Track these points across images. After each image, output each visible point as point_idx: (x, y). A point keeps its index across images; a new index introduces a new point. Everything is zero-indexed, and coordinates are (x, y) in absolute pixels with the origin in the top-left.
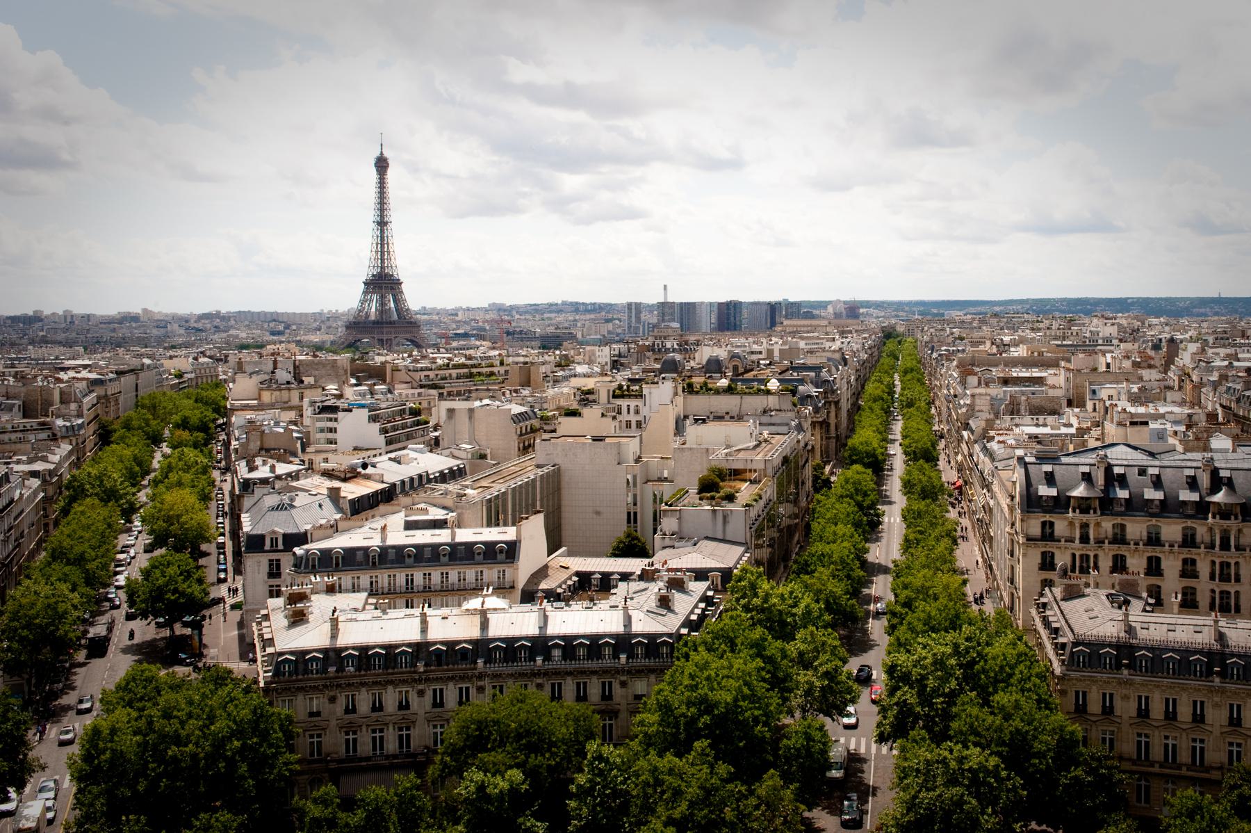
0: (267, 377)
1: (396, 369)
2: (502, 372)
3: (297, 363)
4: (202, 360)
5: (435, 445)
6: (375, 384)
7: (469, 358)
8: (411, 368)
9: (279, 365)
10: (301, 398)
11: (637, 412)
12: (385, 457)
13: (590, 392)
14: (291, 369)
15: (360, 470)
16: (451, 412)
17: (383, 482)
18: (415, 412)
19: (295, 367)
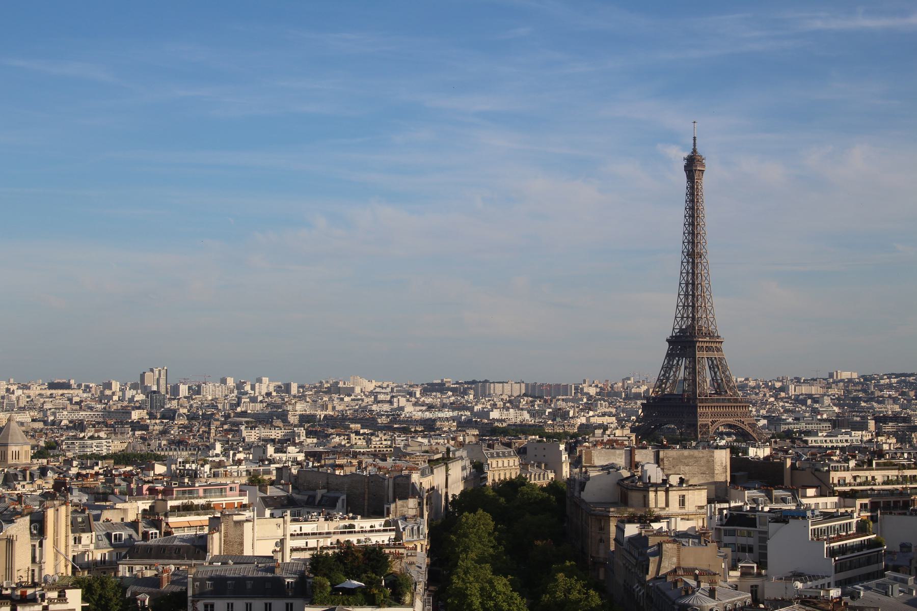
10: (682, 502)
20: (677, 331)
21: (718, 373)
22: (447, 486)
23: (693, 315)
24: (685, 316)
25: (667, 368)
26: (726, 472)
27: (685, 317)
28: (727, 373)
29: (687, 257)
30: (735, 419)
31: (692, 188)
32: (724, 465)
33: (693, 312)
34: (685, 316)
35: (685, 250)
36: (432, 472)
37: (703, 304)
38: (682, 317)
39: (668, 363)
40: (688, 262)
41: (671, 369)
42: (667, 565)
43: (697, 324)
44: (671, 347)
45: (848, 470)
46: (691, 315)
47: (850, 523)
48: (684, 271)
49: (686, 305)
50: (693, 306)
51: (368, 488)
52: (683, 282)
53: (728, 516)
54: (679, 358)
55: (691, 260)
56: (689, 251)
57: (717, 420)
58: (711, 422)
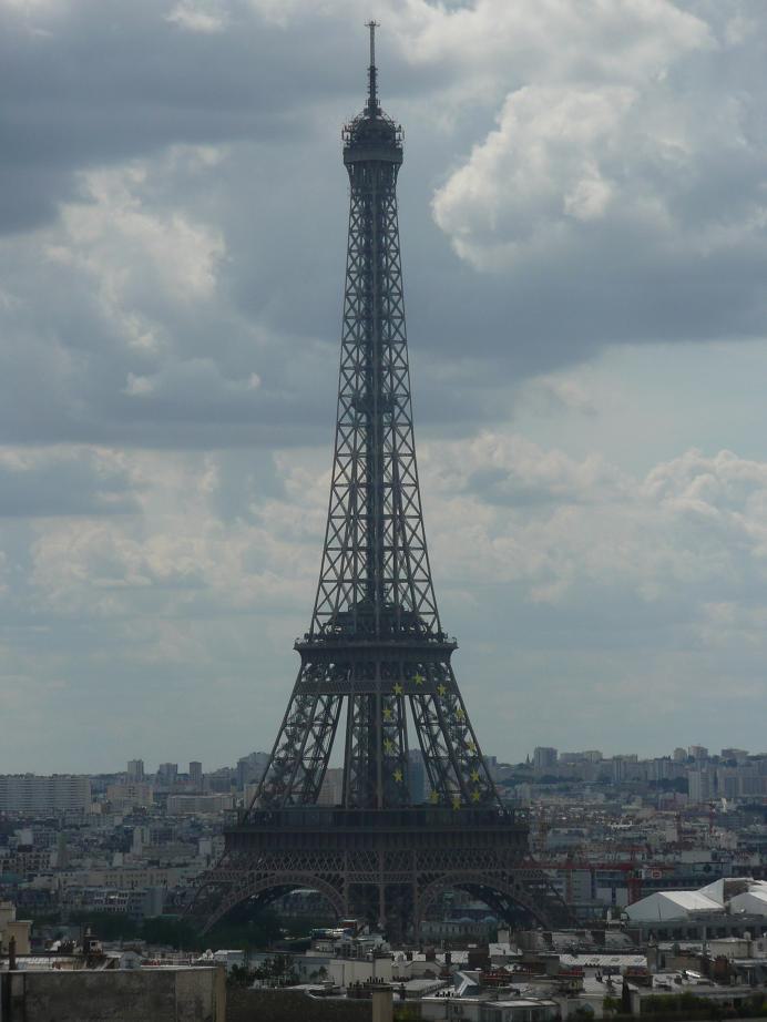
3: (16, 984)
20: (323, 619)
21: (441, 740)
23: (370, 574)
24: (348, 575)
25: (296, 726)
27: (348, 581)
28: (468, 738)
29: (352, 410)
30: (487, 871)
31: (366, 213)
32: (205, 1016)
33: (370, 566)
34: (348, 575)
35: (348, 391)
37: (400, 544)
38: (340, 581)
39: (301, 711)
41: (308, 727)
43: (383, 598)
44: (309, 665)
46: (364, 575)
49: (350, 544)
50: (369, 551)
52: (342, 480)
54: (330, 696)
55: (364, 420)
56: (357, 391)
57: (437, 876)
58: (419, 880)
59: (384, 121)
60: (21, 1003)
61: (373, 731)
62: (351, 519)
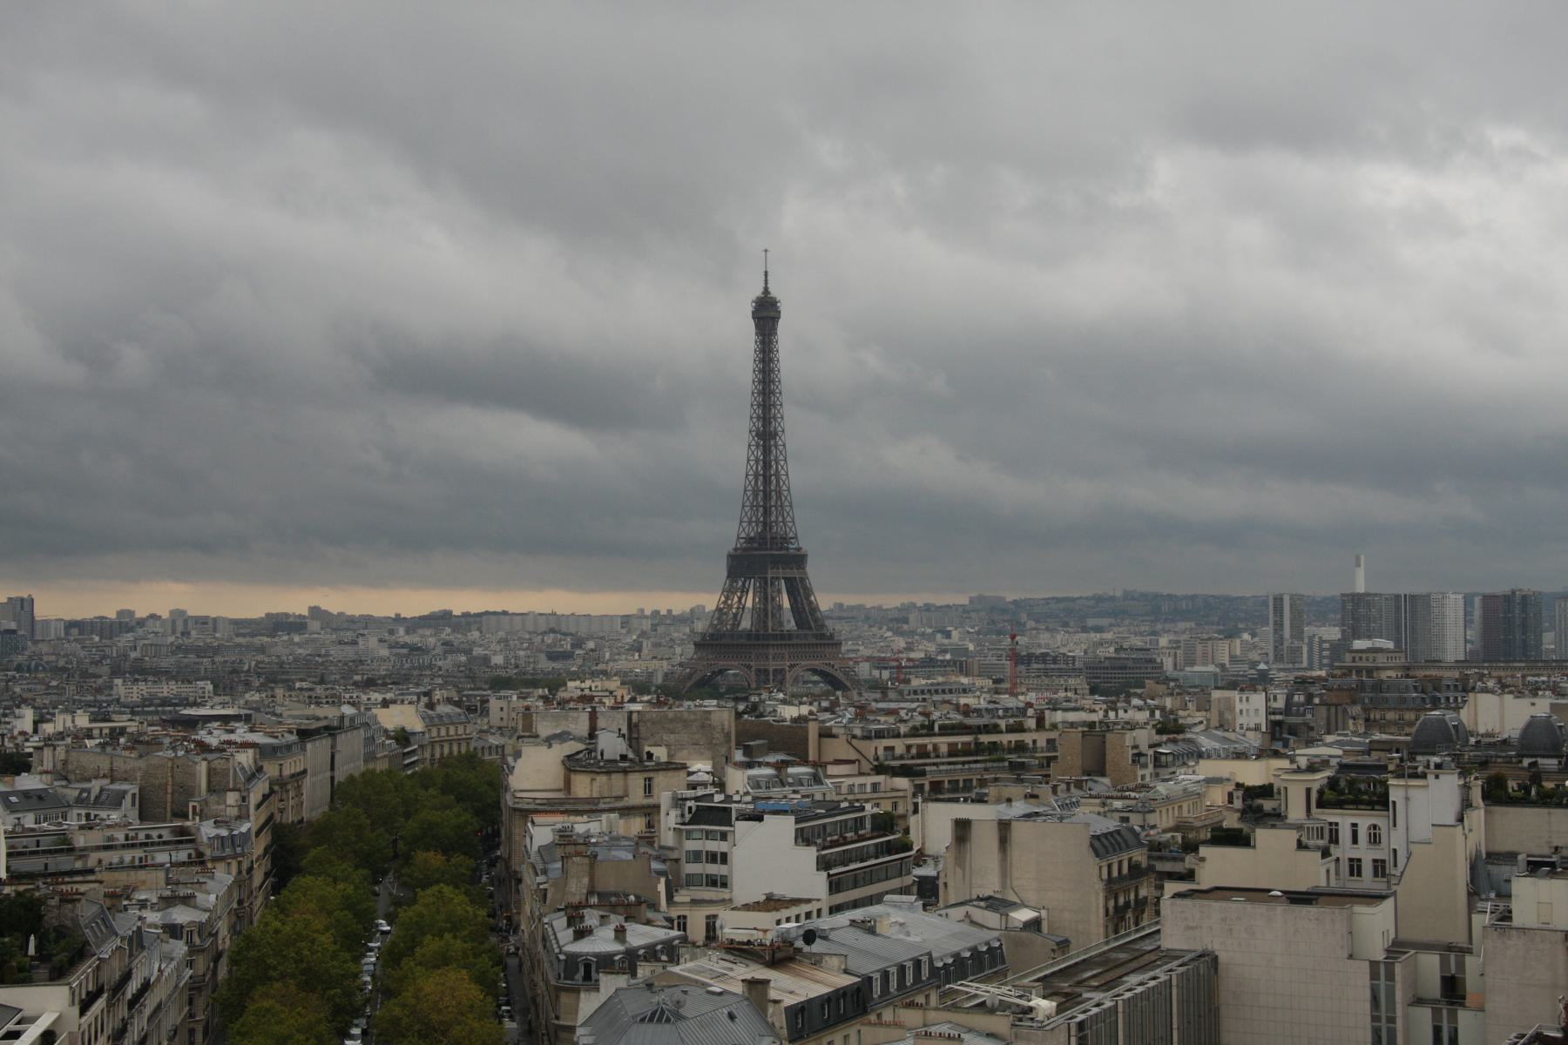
0: (581, 747)
1: (826, 734)
2: (1042, 743)
3: (635, 718)
4: (443, 709)
5: (928, 892)
6: (786, 764)
7: (966, 711)
8: (858, 732)
9: (601, 723)
10: (648, 789)
11: (1375, 839)
12: (843, 918)
13: (1266, 791)
14: (625, 730)
15: (800, 943)
16: (962, 829)
17: (846, 972)
18: (885, 823)
19: (631, 726)
20: (742, 541)
21: (799, 599)
22: (332, 768)
24: (754, 519)
26: (729, 741)
31: (763, 342)
34: (754, 519)
36: (304, 749)
38: (750, 522)
39: (731, 585)
40: (757, 446)
42: (573, 890)
43: (770, 530)
45: (898, 736)
47: (861, 817)
48: (752, 458)
50: (765, 507)
51: (172, 776)
52: (751, 472)
53: (694, 810)
56: (758, 429)
59: (771, 298)
60: (637, 725)
61: (765, 597)
62: (755, 492)
